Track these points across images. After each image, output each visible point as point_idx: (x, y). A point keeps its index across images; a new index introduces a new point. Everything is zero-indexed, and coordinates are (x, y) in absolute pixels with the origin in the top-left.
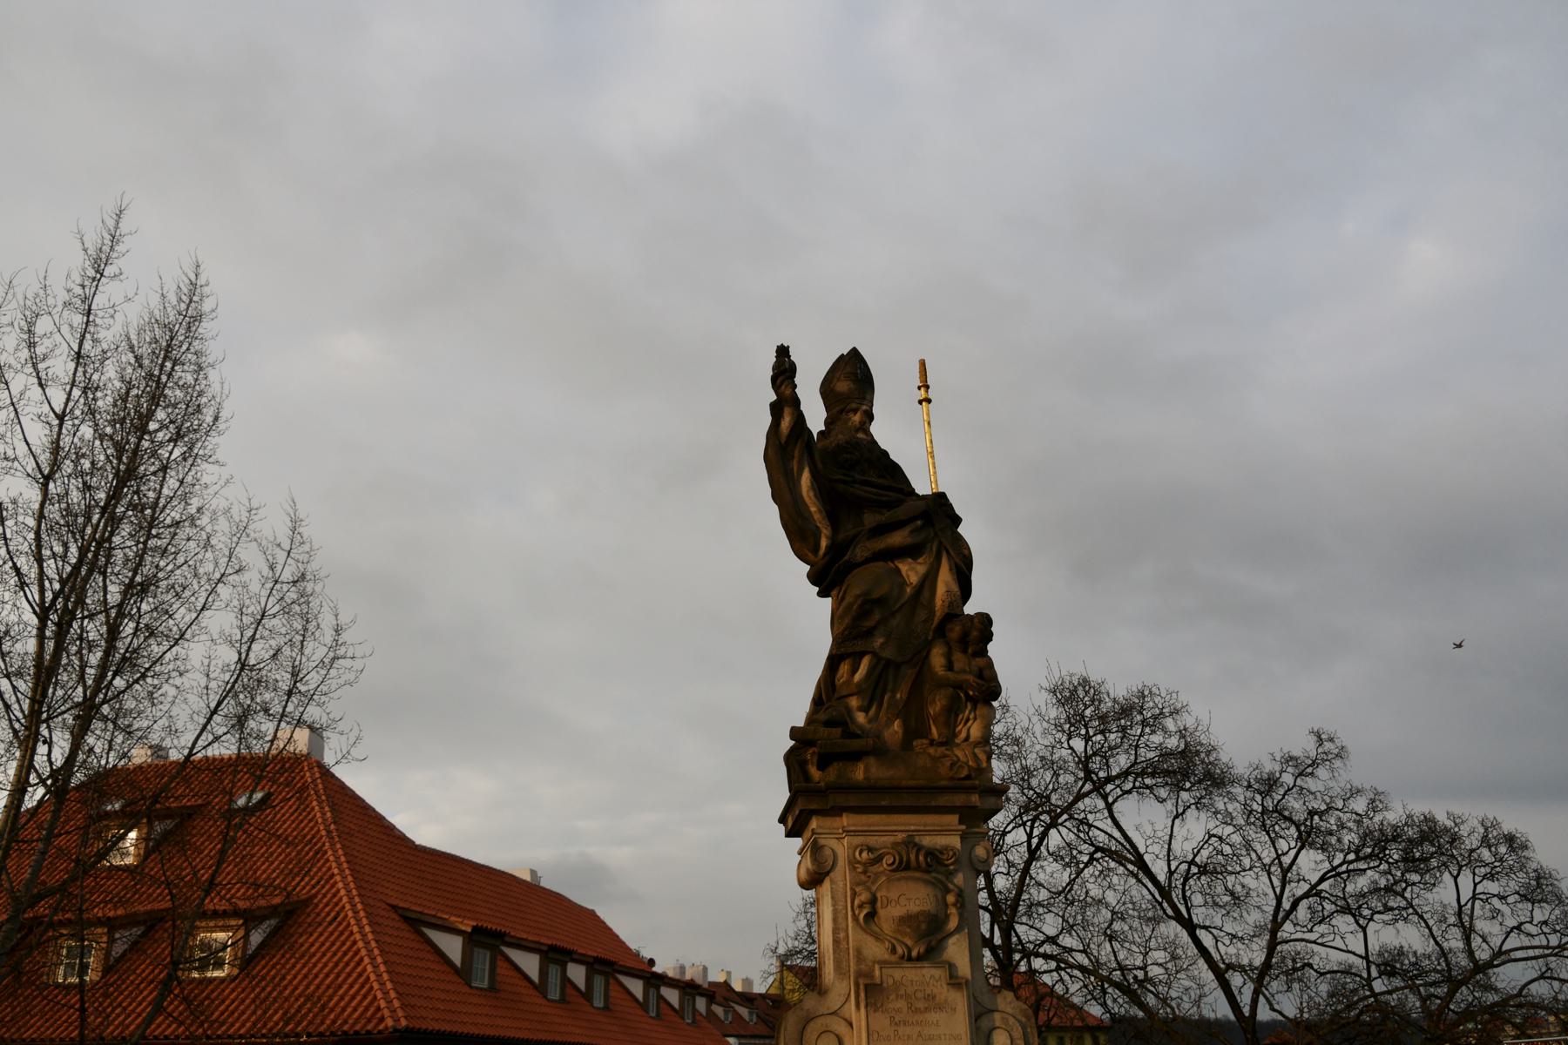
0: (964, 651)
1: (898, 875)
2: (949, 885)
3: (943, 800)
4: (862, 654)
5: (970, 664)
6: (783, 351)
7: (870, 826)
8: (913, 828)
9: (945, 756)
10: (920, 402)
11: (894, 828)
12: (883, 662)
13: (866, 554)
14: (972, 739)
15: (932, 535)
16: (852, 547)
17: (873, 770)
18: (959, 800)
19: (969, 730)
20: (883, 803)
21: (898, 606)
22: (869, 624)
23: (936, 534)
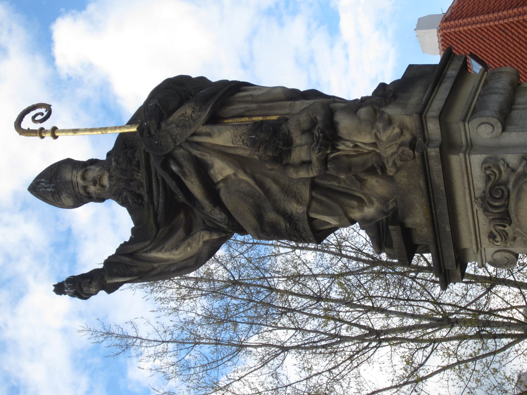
0: (289, 152)
1: (514, 220)
2: (519, 170)
3: (438, 180)
4: (311, 220)
5: (301, 145)
6: (59, 289)
7: (469, 229)
8: (468, 199)
9: (394, 164)
10: (55, 137)
11: (470, 213)
12: (314, 194)
13: (217, 211)
14: (374, 141)
15: (181, 151)
16: (216, 223)
17: (418, 220)
18: (436, 166)
19: (365, 144)
20: (448, 229)
21: (257, 188)
22: (283, 224)
23: (180, 146)
